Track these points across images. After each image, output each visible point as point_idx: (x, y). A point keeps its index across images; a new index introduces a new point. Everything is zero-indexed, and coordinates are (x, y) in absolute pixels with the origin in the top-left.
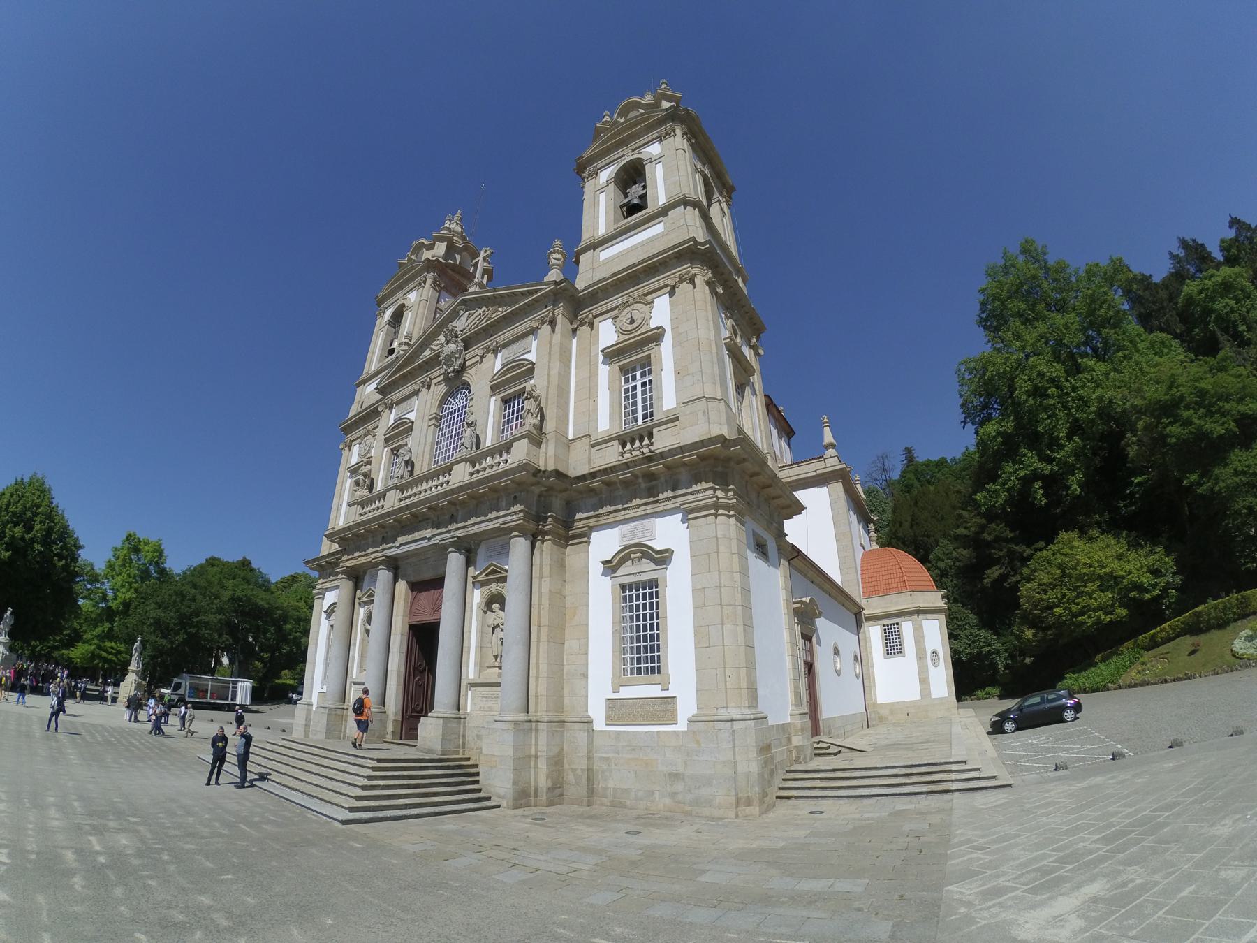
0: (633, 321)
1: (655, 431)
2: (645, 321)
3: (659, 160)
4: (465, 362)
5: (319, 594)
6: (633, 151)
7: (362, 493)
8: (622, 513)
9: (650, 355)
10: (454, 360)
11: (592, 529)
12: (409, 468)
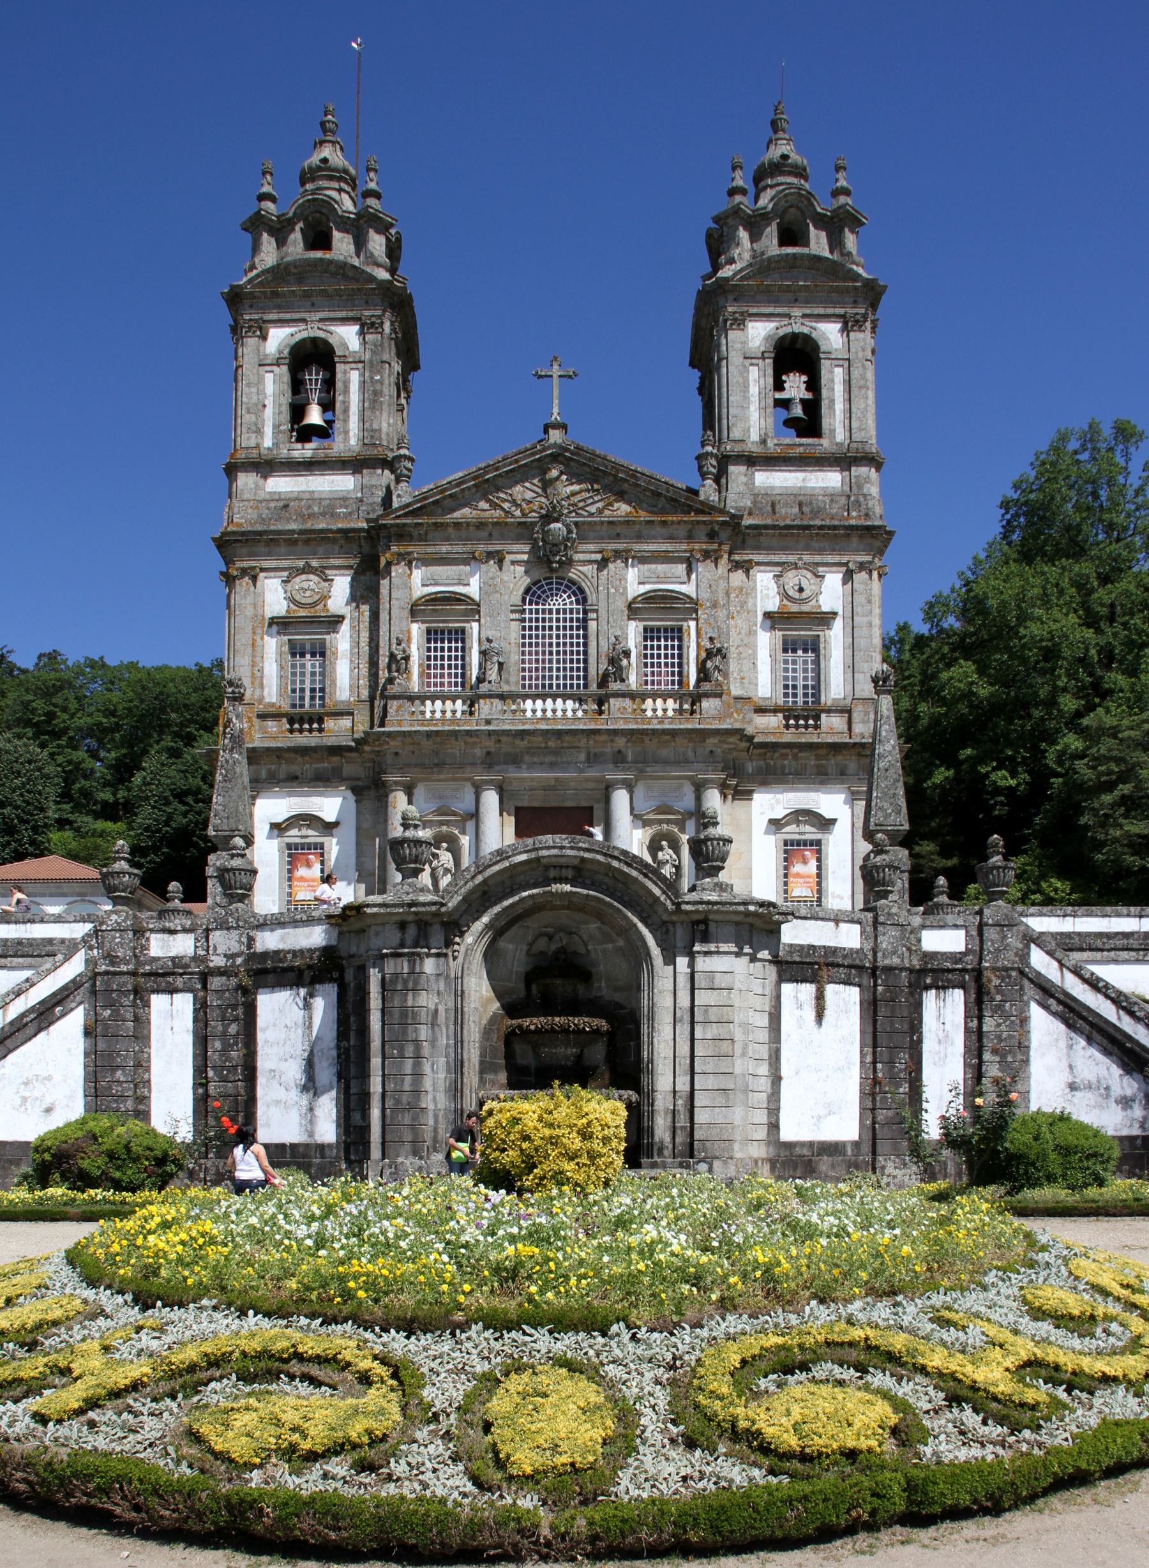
0: (801, 590)
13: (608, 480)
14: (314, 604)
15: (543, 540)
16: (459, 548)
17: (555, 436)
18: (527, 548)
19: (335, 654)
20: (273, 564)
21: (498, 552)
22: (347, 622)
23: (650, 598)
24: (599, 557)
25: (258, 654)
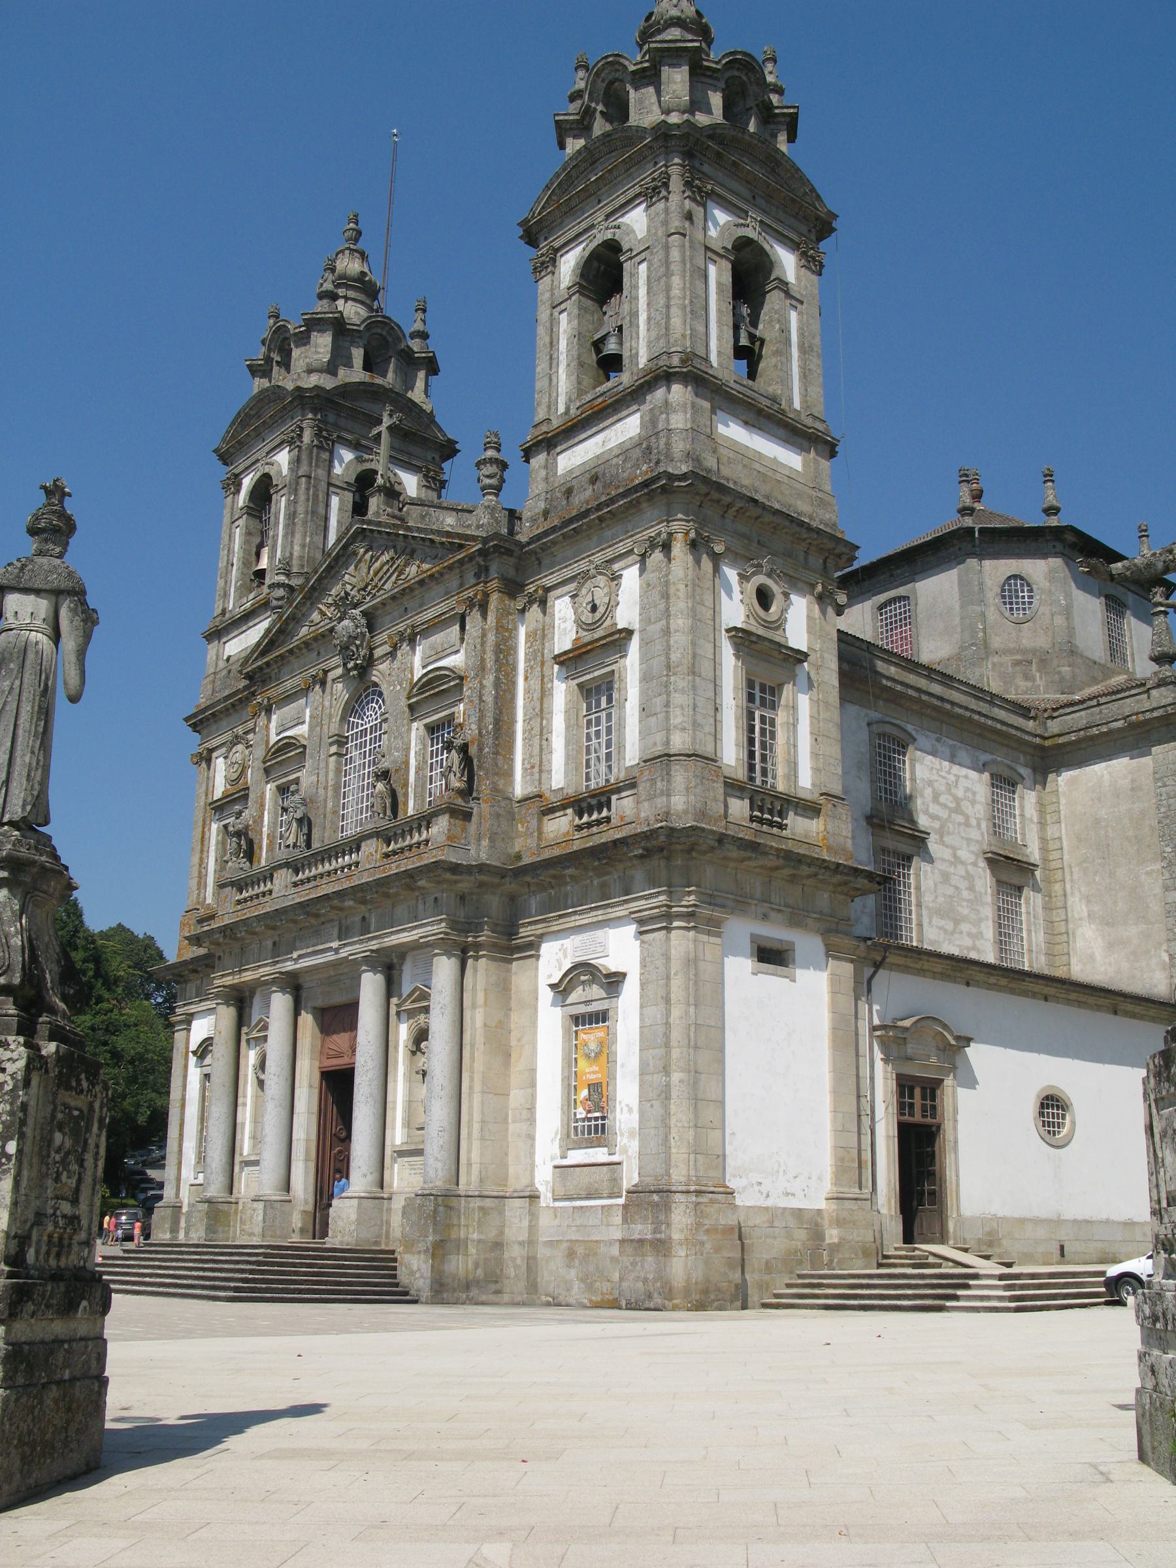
0: (594, 608)
1: (614, 798)
2: (611, 606)
3: (643, 255)
4: (371, 650)
5: (181, 1022)
6: (608, 217)
7: (238, 867)
8: (573, 918)
9: (613, 671)
11: (541, 937)
12: (305, 830)
14: (239, 778)
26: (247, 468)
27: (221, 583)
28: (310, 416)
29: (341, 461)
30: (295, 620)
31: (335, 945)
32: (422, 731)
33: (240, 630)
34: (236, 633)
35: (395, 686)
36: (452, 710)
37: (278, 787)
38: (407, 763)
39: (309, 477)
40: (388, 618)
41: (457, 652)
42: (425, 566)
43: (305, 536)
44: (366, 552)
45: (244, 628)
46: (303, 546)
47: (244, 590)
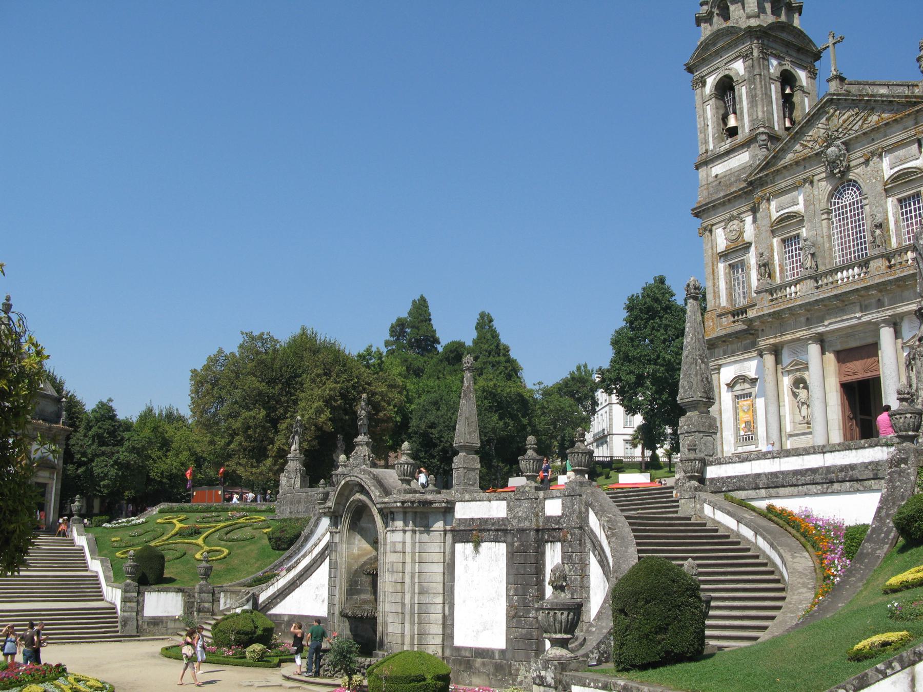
10: (839, 162)
13: (862, 105)
15: (827, 160)
16: (790, 182)
17: (833, 86)
18: (823, 169)
19: (749, 267)
20: (717, 220)
21: (808, 178)
22: (753, 245)
23: (896, 178)
24: (862, 160)
25: (716, 278)
26: (709, 73)
27: (701, 136)
28: (755, 41)
29: (772, 66)
30: (784, 151)
31: (858, 315)
32: (896, 202)
33: (723, 160)
34: (720, 161)
35: (871, 180)
36: (919, 189)
37: (782, 239)
38: (887, 219)
39: (760, 75)
40: (858, 145)
41: (918, 158)
42: (884, 115)
43: (763, 107)
44: (836, 111)
45: (726, 159)
46: (763, 112)
47: (719, 140)
